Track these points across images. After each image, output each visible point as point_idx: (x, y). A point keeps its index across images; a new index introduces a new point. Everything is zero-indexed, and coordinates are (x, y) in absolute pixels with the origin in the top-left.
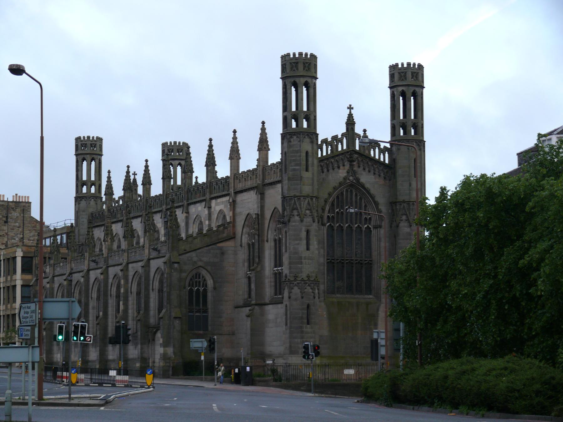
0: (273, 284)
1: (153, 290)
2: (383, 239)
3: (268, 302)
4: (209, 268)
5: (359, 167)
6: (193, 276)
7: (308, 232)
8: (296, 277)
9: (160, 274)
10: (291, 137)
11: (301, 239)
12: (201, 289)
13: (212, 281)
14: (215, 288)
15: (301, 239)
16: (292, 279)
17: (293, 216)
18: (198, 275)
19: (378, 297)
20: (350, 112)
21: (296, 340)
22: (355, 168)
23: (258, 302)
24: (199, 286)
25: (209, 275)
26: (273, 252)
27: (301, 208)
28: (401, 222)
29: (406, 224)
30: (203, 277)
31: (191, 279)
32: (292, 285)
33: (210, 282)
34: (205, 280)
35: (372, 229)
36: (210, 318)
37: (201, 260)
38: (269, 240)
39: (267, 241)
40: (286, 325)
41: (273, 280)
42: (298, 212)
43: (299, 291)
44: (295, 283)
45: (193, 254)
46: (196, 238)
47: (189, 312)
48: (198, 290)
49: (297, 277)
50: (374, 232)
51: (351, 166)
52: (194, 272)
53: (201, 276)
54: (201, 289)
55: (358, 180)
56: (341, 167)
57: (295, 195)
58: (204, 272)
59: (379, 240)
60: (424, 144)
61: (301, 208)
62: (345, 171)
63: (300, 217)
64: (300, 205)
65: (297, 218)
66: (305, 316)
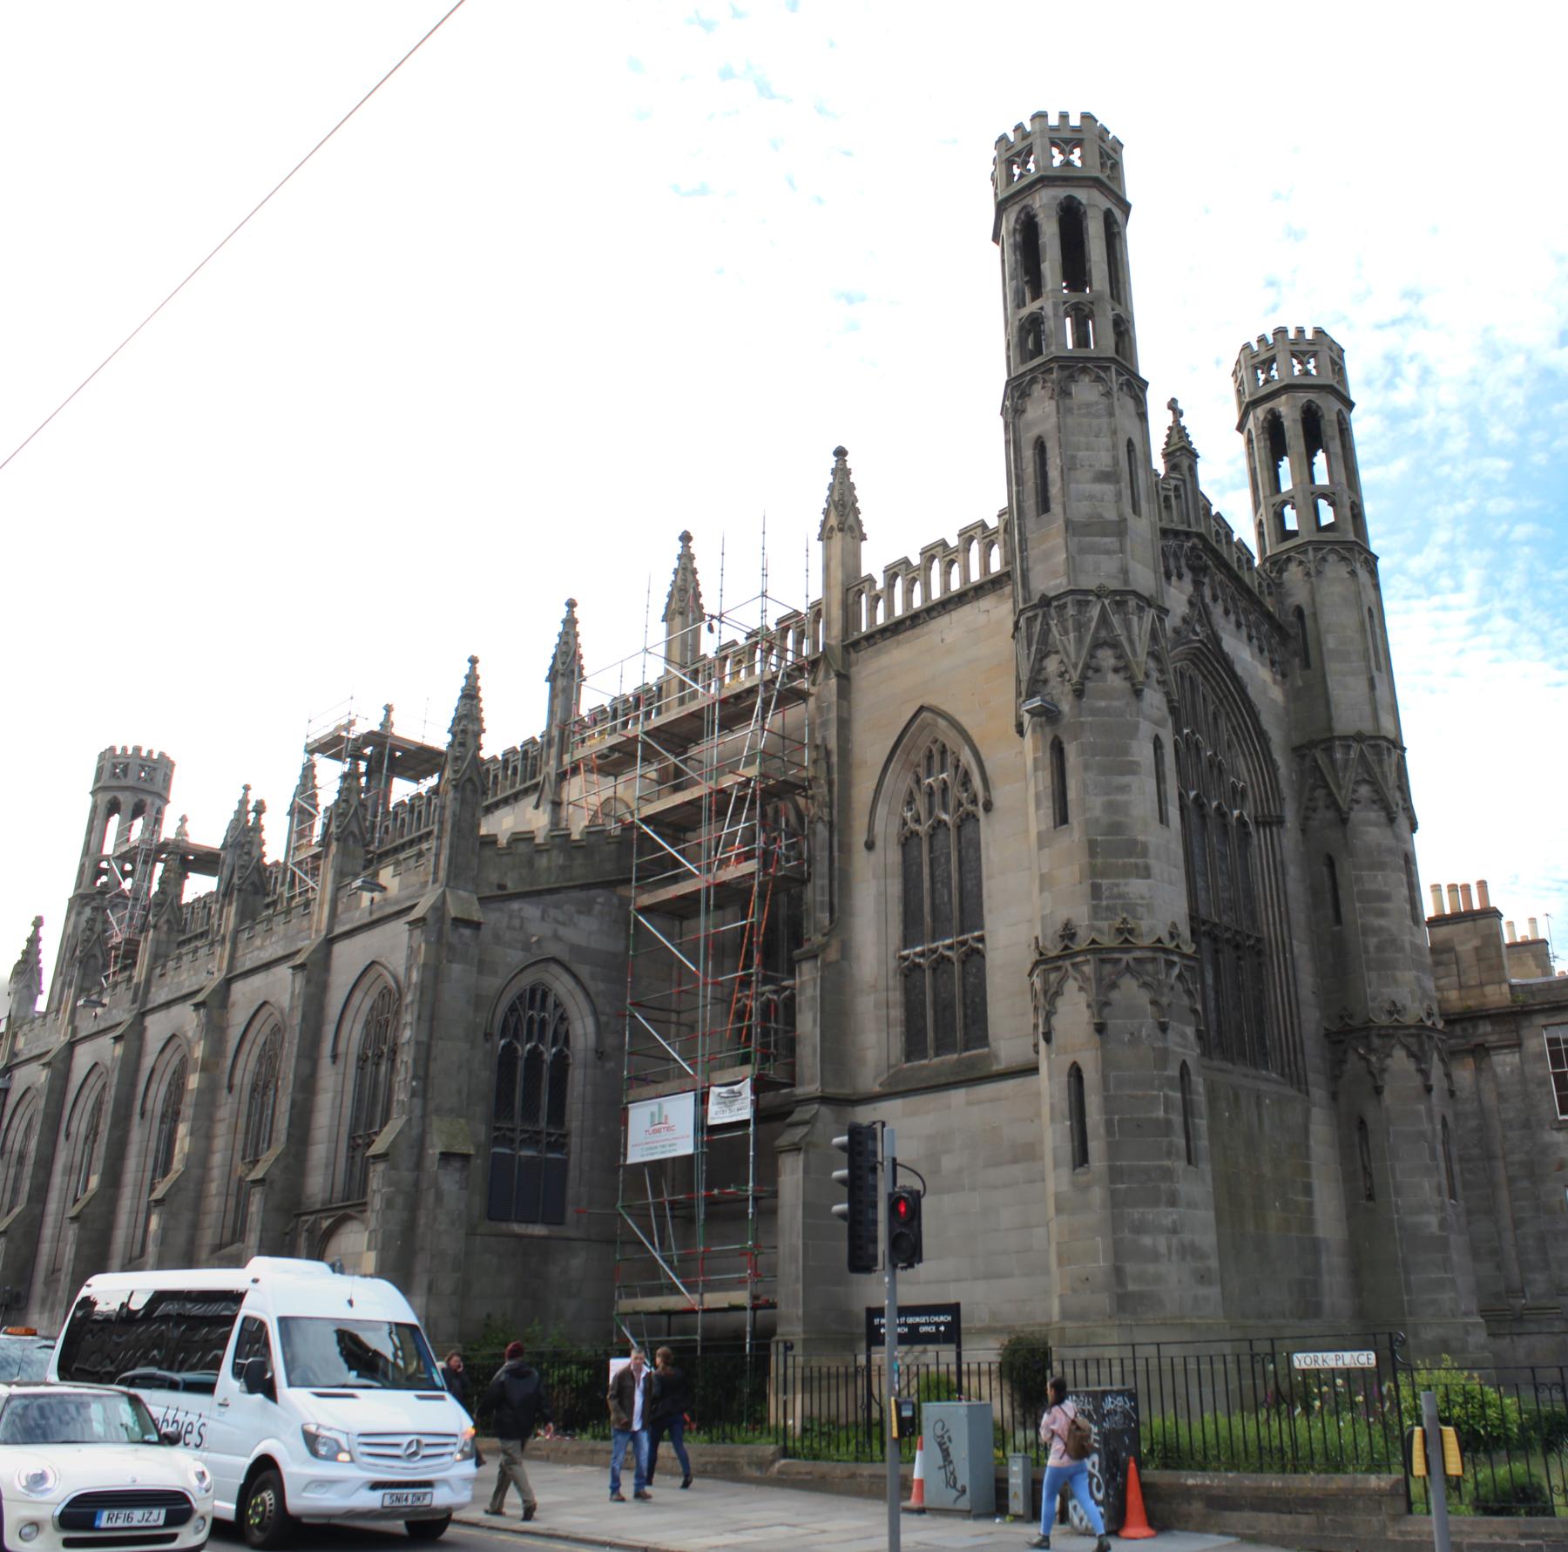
0: (897, 1013)
1: (335, 1057)
2: (1293, 871)
3: (877, 1089)
4: (584, 971)
5: (1215, 598)
6: (520, 997)
7: (1157, 743)
8: (1126, 933)
9: (374, 993)
10: (1072, 378)
11: (1131, 768)
12: (549, 1053)
13: (590, 1022)
14: (600, 1054)
15: (1131, 768)
16: (1107, 941)
17: (1097, 670)
18: (537, 995)
19: (1299, 1082)
20: (1176, 421)
21: (1147, 1240)
22: (1208, 600)
23: (831, 1091)
24: (541, 1038)
25: (580, 997)
26: (895, 888)
27: (1131, 642)
28: (1356, 807)
29: (1375, 815)
30: (557, 1005)
31: (512, 1009)
32: (1108, 968)
33: (583, 1030)
34: (563, 1018)
35: (1252, 828)
36: (573, 1173)
37: (557, 937)
38: (879, 843)
39: (870, 846)
40: (1081, 1157)
41: (897, 996)
42: (1119, 657)
43: (1143, 997)
44: (1126, 957)
45: (530, 910)
46: (539, 850)
47: (496, 1141)
48: (535, 1055)
49: (1131, 931)
50: (1258, 837)
51: (1197, 584)
52: (527, 980)
53: (550, 1001)
54: (549, 1053)
55: (1217, 640)
56: (1174, 579)
57: (1101, 587)
58: (562, 985)
59: (1280, 869)
60: (1373, 573)
61: (1131, 642)
62: (1184, 598)
63: (1130, 678)
64: (1127, 626)
65: (1115, 681)
66: (1177, 1119)
